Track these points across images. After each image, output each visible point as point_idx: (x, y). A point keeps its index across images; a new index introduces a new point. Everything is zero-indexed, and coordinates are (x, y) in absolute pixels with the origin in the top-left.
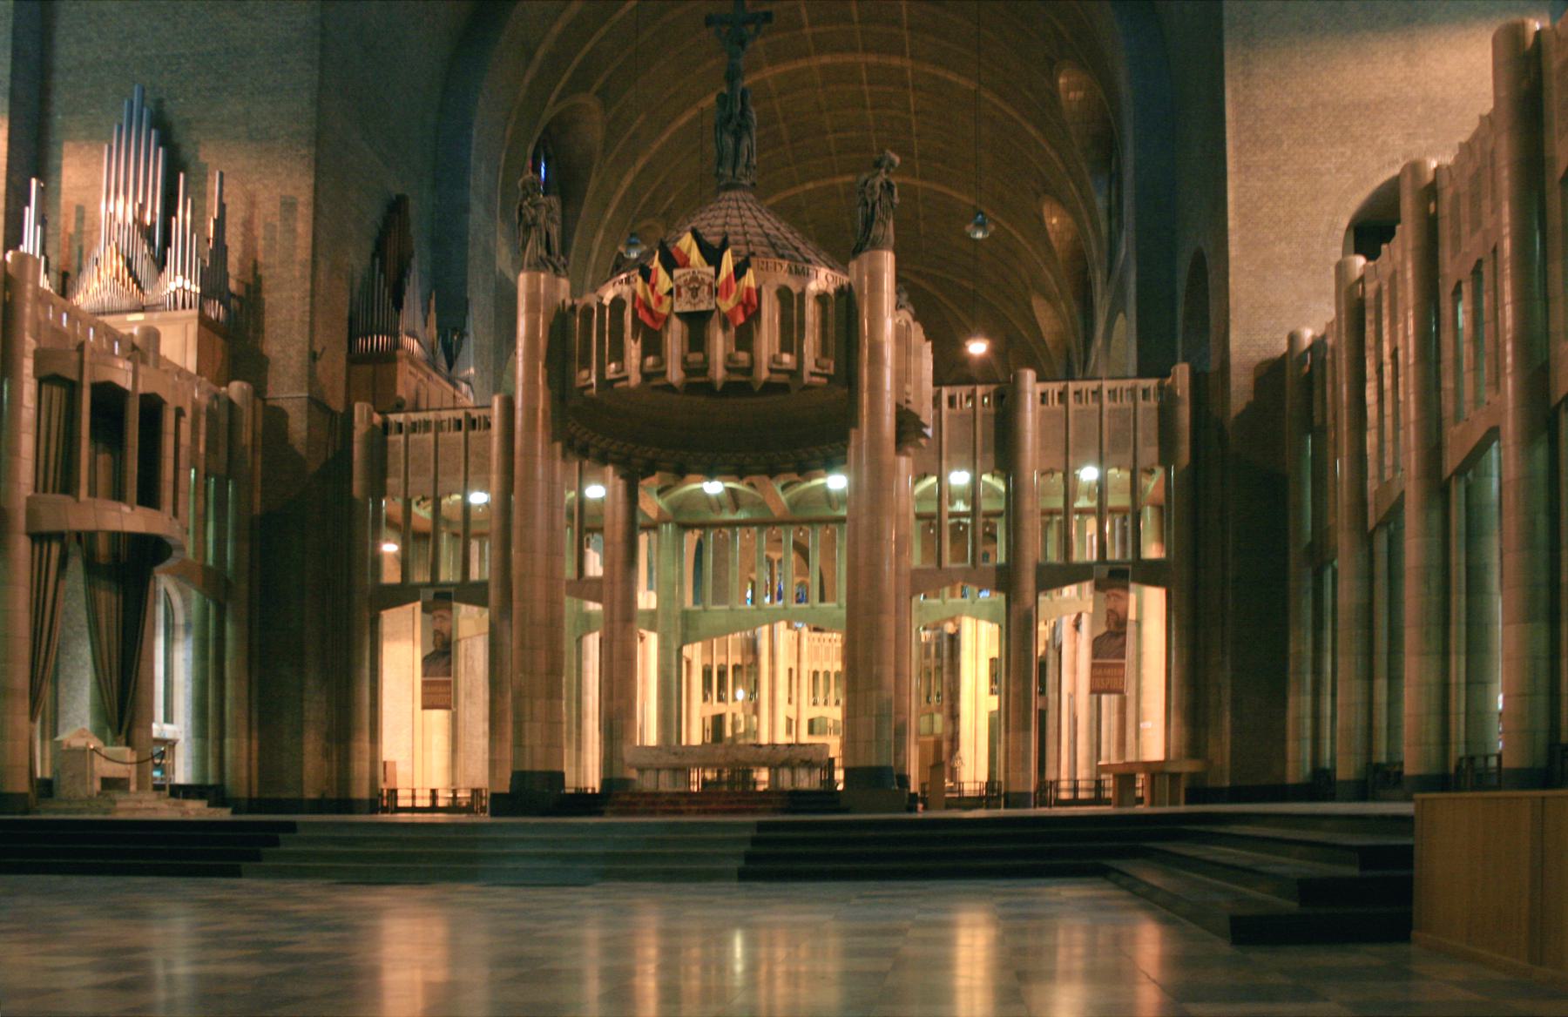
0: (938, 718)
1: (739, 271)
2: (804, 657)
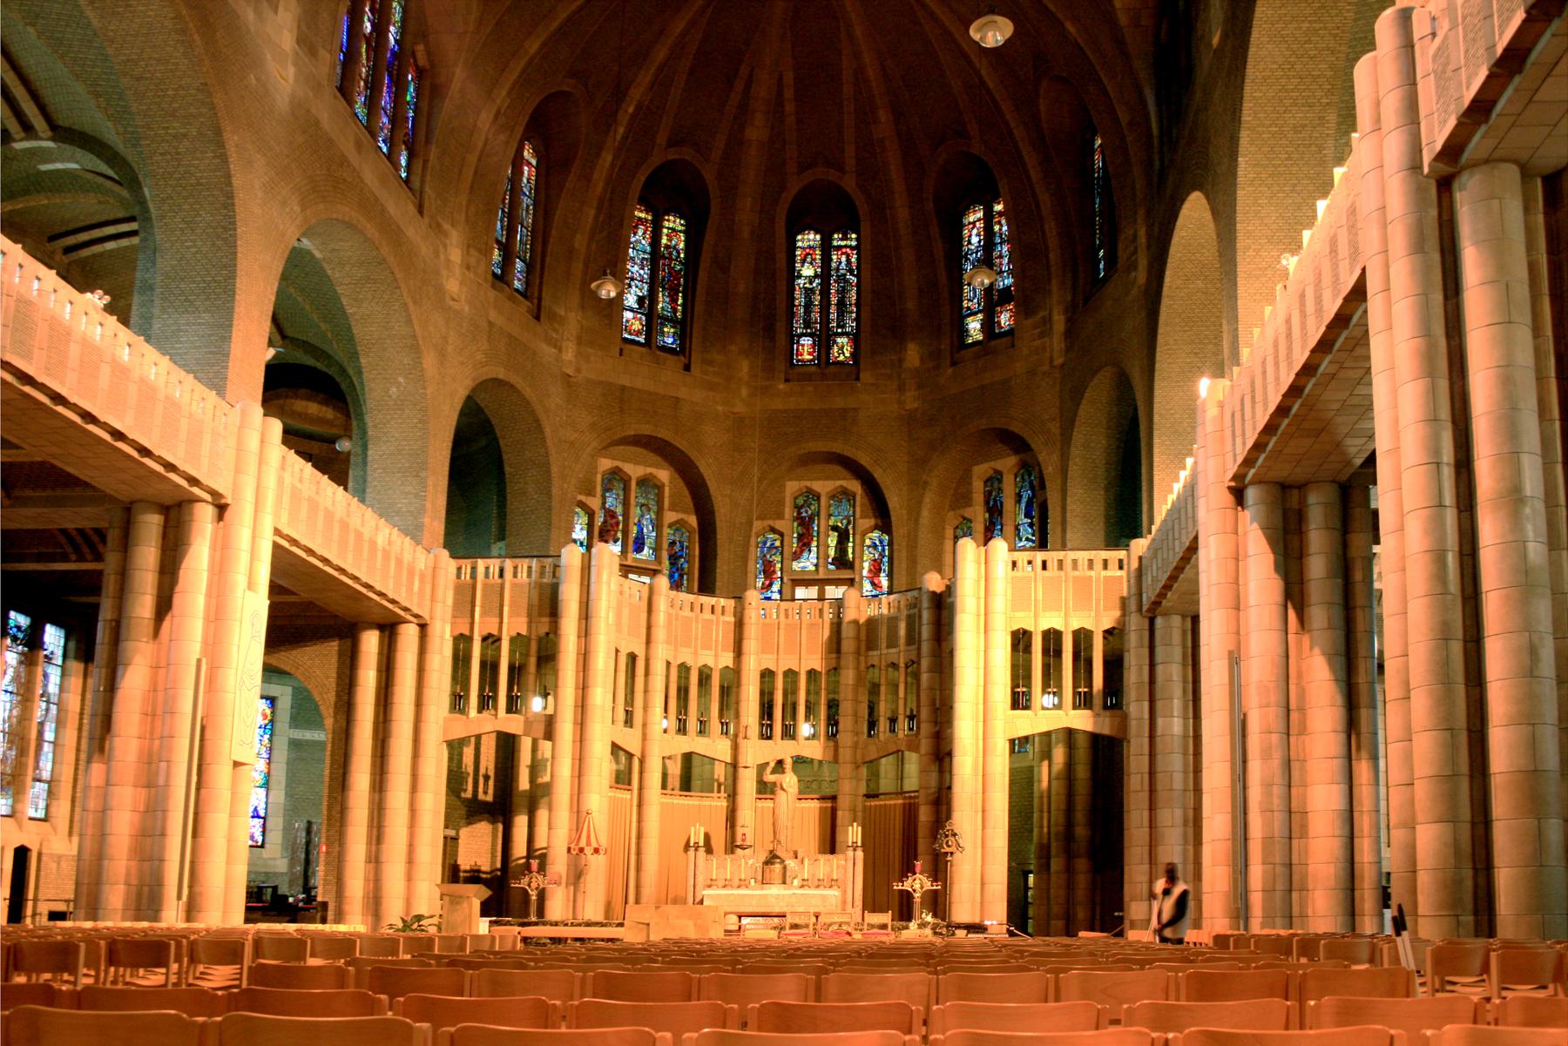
0: (913, 764)
2: (660, 634)
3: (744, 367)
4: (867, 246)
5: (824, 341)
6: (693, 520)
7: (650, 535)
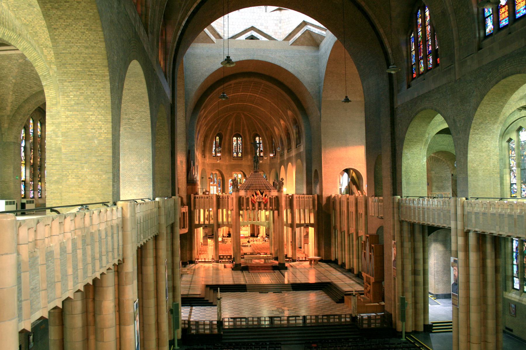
1: (265, 196)
3: (227, 158)
4: (243, 139)
5: (237, 153)
6: (221, 178)
7: (216, 180)
